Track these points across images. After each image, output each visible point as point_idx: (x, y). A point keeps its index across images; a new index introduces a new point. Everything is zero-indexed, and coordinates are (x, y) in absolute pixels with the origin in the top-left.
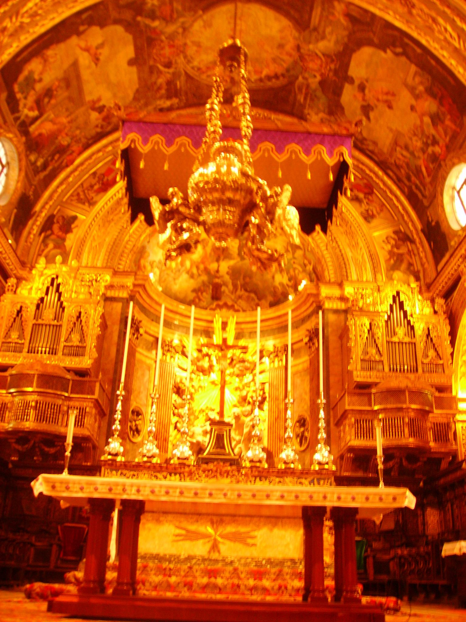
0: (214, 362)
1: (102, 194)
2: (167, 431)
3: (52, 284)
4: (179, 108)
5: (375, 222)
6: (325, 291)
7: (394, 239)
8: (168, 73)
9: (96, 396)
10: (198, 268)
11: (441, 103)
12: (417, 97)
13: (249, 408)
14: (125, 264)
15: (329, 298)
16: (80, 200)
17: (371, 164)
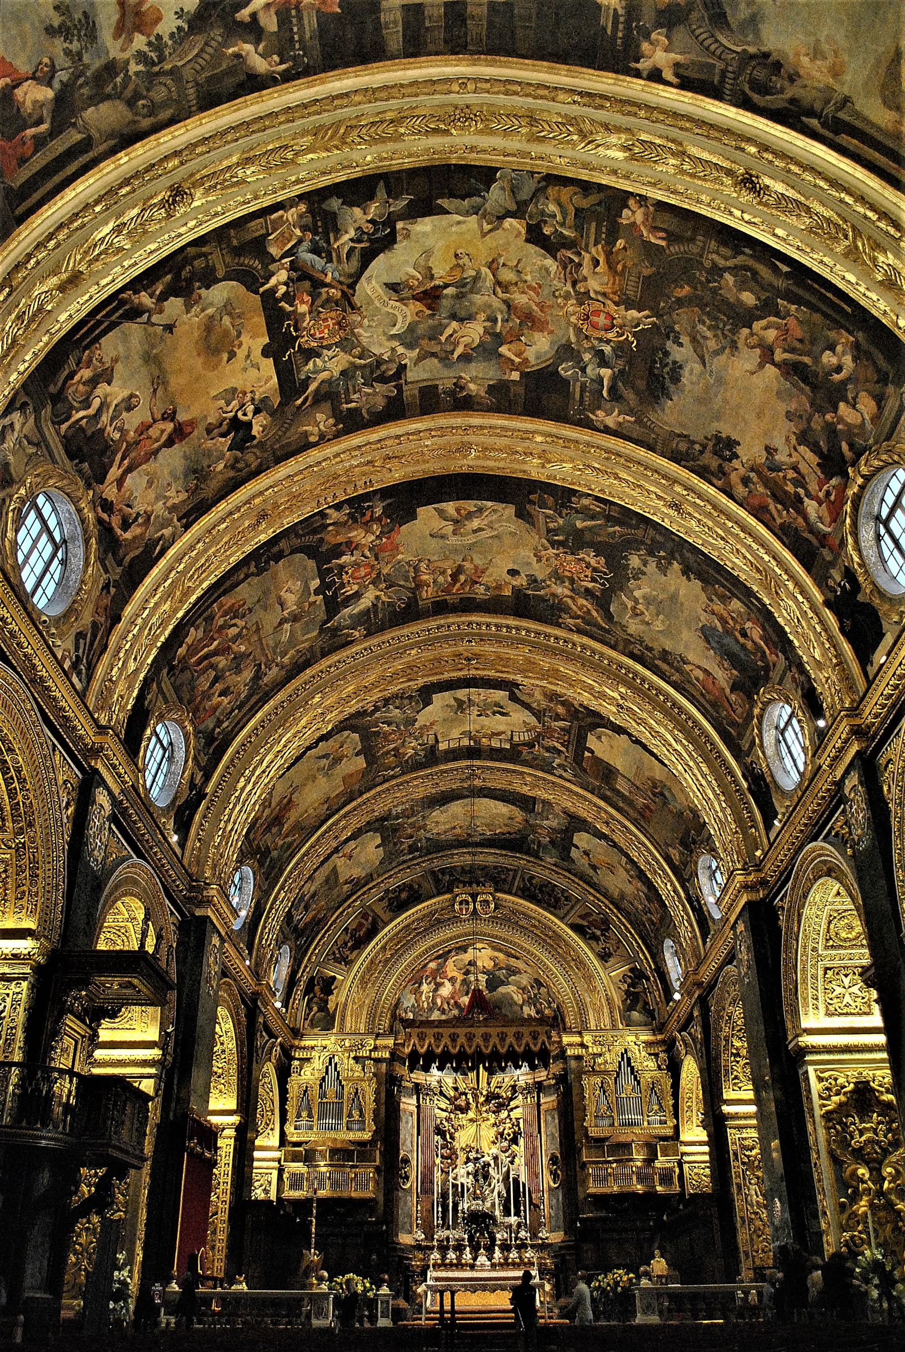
0: (471, 1101)
1: (356, 952)
2: (432, 1173)
3: (330, 1064)
4: (420, 856)
5: (612, 961)
6: (566, 1039)
7: (630, 977)
8: (410, 841)
9: (377, 1163)
10: (448, 1003)
11: (649, 888)
12: (631, 876)
13: (505, 1144)
14: (386, 1023)
15: (570, 1045)
16: (336, 960)
17: (607, 902)
